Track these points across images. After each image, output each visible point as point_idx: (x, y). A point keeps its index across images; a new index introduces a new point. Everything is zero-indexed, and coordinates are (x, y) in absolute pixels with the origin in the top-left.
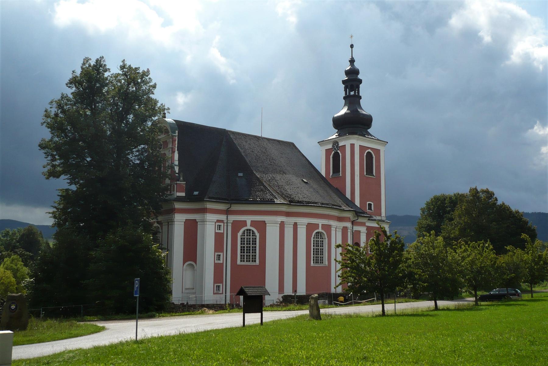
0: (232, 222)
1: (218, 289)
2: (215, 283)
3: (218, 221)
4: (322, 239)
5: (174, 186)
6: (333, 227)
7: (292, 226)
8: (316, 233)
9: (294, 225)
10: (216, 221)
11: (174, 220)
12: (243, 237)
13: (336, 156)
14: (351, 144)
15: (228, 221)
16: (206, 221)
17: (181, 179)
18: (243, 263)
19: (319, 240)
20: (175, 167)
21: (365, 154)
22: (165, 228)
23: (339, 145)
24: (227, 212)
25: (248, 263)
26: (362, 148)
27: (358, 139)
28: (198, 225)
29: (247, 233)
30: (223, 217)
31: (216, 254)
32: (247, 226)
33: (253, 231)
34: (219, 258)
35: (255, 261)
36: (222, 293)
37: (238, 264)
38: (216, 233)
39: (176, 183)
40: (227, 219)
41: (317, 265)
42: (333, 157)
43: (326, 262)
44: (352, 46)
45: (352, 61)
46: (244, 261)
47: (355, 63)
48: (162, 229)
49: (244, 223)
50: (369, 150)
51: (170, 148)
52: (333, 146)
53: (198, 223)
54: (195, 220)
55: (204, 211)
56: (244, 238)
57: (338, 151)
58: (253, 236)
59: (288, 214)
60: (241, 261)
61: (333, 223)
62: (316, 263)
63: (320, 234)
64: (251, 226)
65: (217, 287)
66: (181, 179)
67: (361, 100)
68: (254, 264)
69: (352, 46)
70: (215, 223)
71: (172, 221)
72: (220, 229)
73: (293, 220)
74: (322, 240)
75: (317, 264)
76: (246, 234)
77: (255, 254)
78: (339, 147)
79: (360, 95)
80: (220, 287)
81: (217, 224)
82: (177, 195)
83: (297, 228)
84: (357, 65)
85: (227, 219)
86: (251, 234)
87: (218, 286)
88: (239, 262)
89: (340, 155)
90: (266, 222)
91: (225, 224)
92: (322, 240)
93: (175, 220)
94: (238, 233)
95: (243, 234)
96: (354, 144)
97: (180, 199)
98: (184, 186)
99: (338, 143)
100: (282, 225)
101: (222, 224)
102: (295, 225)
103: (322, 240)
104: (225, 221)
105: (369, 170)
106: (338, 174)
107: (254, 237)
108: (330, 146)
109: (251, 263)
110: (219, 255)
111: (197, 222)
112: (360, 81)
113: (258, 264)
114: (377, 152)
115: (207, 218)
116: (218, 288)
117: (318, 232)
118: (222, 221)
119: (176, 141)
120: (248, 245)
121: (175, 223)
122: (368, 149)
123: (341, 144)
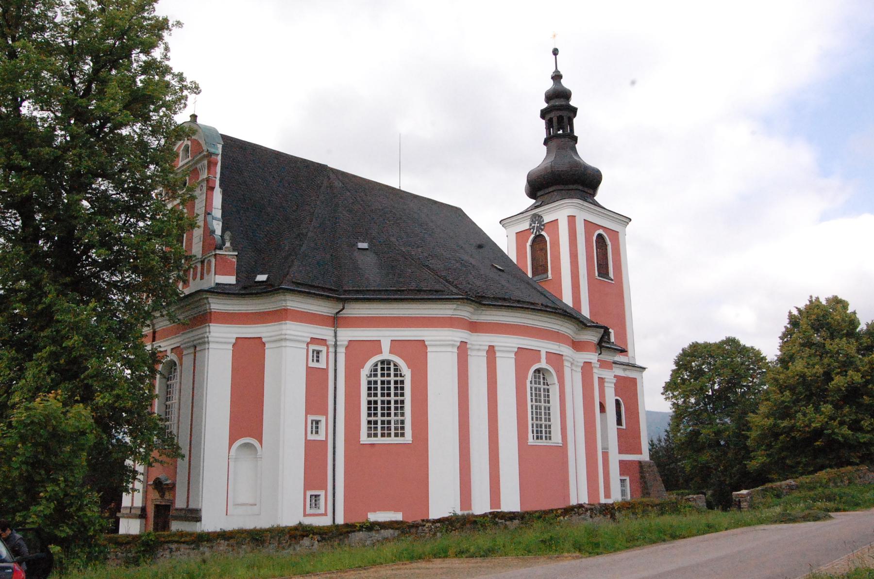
0: (346, 343)
1: (316, 505)
2: (307, 487)
3: (314, 340)
4: (548, 385)
5: (209, 262)
6: (567, 360)
7: (485, 354)
8: (535, 372)
9: (488, 352)
10: (309, 340)
11: (208, 337)
12: (373, 379)
13: (539, 241)
14: (568, 216)
15: (338, 343)
16: (286, 339)
17: (228, 244)
18: (373, 440)
19: (542, 386)
20: (215, 222)
21: (595, 238)
22: (187, 361)
23: (543, 221)
24: (336, 321)
25: (386, 440)
26: (589, 226)
27: (581, 208)
28: (266, 351)
29: (383, 369)
30: (325, 332)
31: (311, 418)
32: (381, 353)
33: (395, 365)
34: (317, 428)
35: (403, 435)
36: (325, 514)
37: (361, 443)
38: (309, 370)
39: (213, 253)
40: (336, 336)
41: (539, 443)
42: (532, 246)
43: (557, 438)
44: (555, 52)
45: (557, 77)
46: (376, 435)
47: (562, 81)
48: (181, 365)
49: (376, 346)
50: (601, 231)
51: (203, 180)
52: (531, 225)
53: (267, 346)
54: (260, 338)
55: (281, 315)
56: (376, 382)
57: (543, 233)
58: (396, 375)
59: (474, 327)
60: (369, 436)
61: (566, 351)
62: (537, 438)
63: (543, 375)
64: (391, 352)
65: (314, 497)
66: (228, 244)
67: (576, 145)
68: (399, 440)
69: (555, 52)
70: (308, 344)
71: (204, 343)
72: (318, 361)
73: (483, 340)
74: (548, 387)
75: (539, 441)
76: (379, 372)
77: (402, 418)
78: (543, 225)
79: (576, 134)
80: (319, 500)
81: (312, 347)
82: (218, 281)
83: (495, 358)
84: (566, 83)
85: (336, 336)
86: (392, 372)
87: (316, 496)
88: (364, 438)
89: (548, 239)
90: (426, 343)
91: (332, 350)
92: (548, 387)
93: (210, 339)
94: (361, 370)
95: (373, 373)
96: (575, 216)
97: (221, 291)
98: (234, 260)
99: (542, 217)
100: (463, 349)
101: (323, 349)
102: (491, 351)
103: (546, 387)
104: (331, 342)
105: (603, 269)
106: (545, 276)
107: (399, 379)
108: (525, 226)
109: (393, 440)
110: (317, 422)
111: (264, 344)
112: (574, 111)
113: (411, 442)
114: (614, 234)
115: (288, 332)
116: (316, 501)
117: (538, 371)
118: (323, 342)
119: (216, 164)
120: (386, 398)
121: (211, 346)
122: (599, 229)
123: (547, 219)
